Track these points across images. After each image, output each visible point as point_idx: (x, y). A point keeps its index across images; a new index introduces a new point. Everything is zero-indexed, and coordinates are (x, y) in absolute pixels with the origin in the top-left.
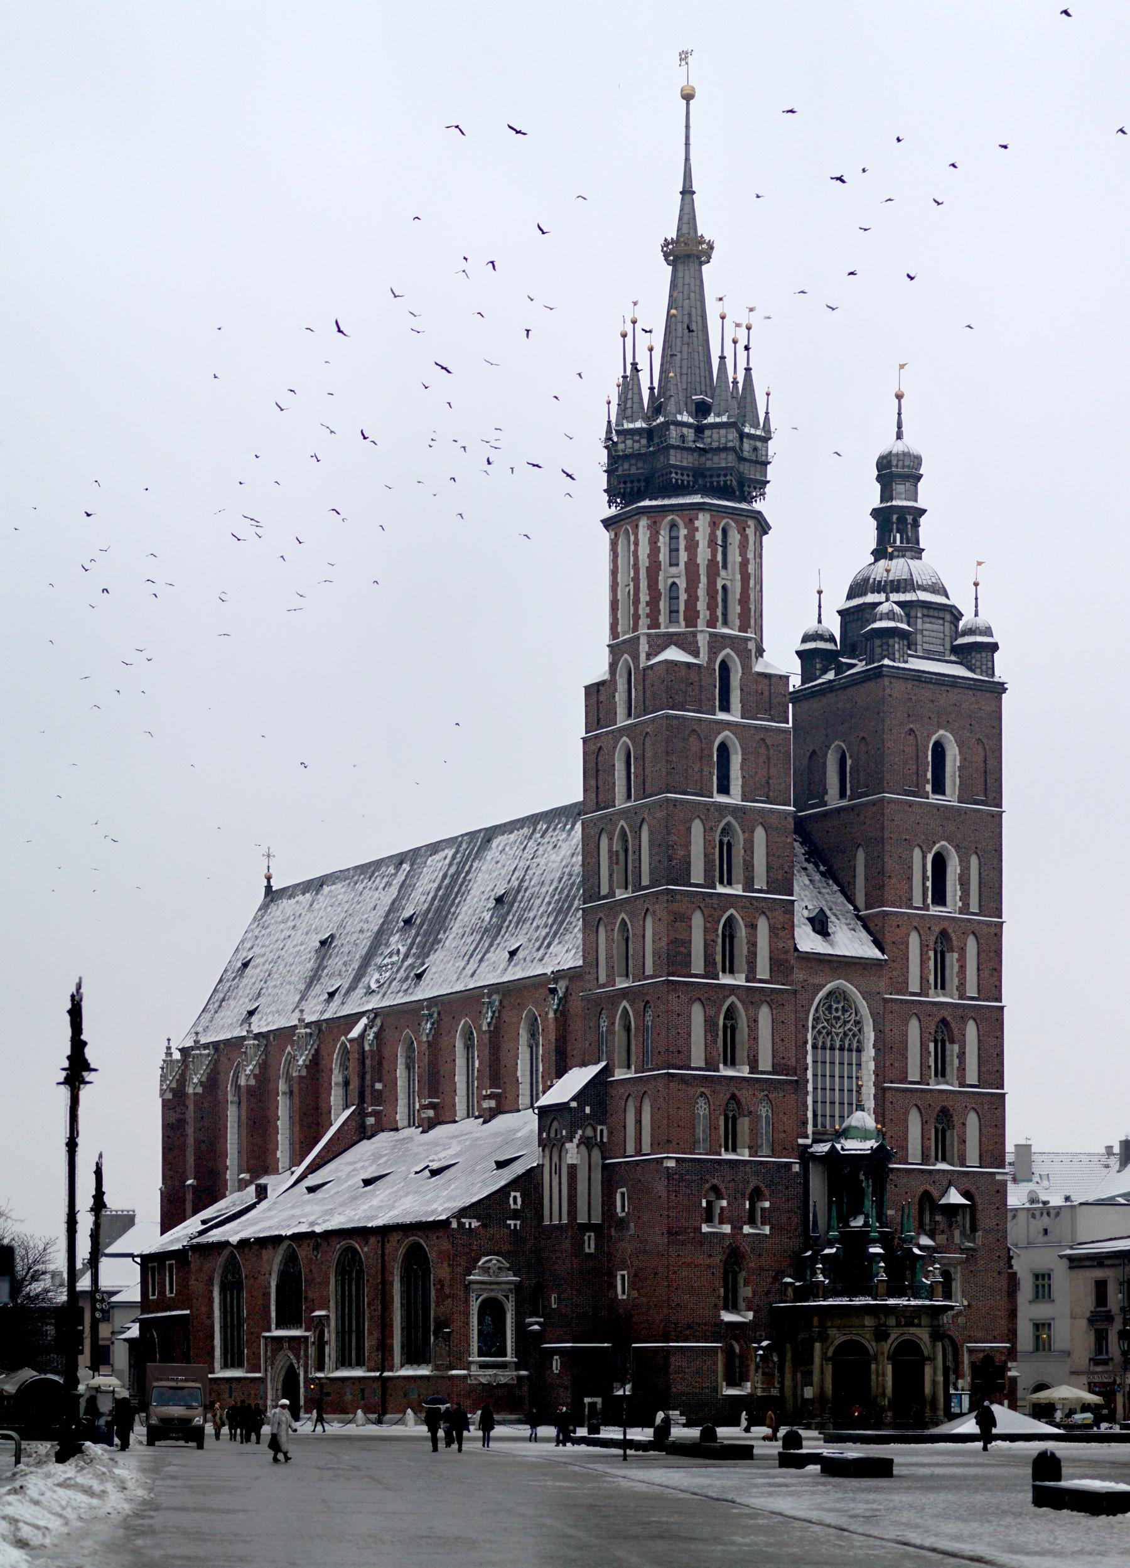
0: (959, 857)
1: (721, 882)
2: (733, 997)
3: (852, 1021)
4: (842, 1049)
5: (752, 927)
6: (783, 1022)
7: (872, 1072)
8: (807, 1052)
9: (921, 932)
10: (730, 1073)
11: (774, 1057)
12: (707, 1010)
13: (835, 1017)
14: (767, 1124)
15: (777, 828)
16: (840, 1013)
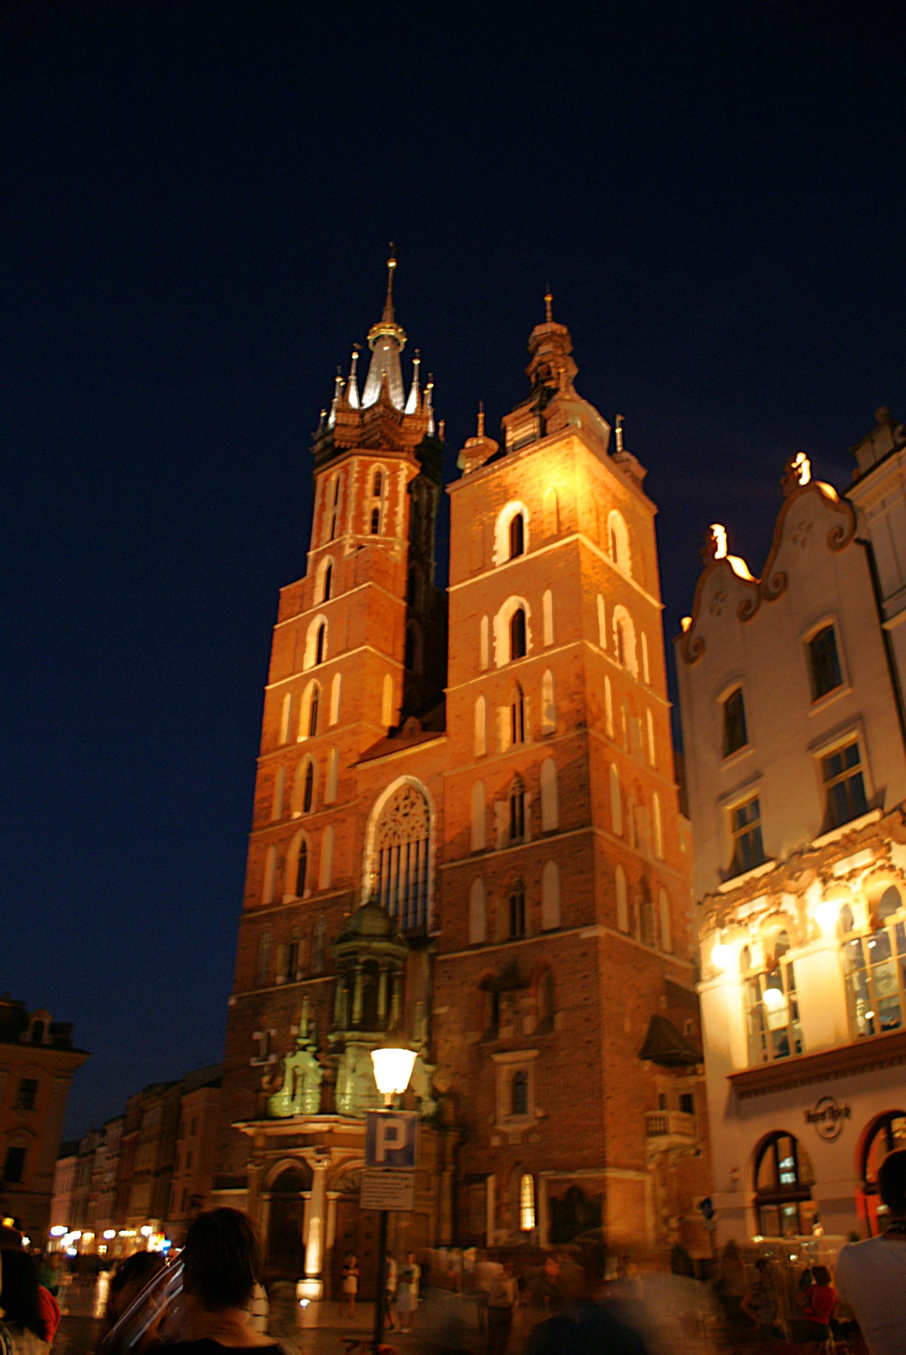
5: (324, 760)
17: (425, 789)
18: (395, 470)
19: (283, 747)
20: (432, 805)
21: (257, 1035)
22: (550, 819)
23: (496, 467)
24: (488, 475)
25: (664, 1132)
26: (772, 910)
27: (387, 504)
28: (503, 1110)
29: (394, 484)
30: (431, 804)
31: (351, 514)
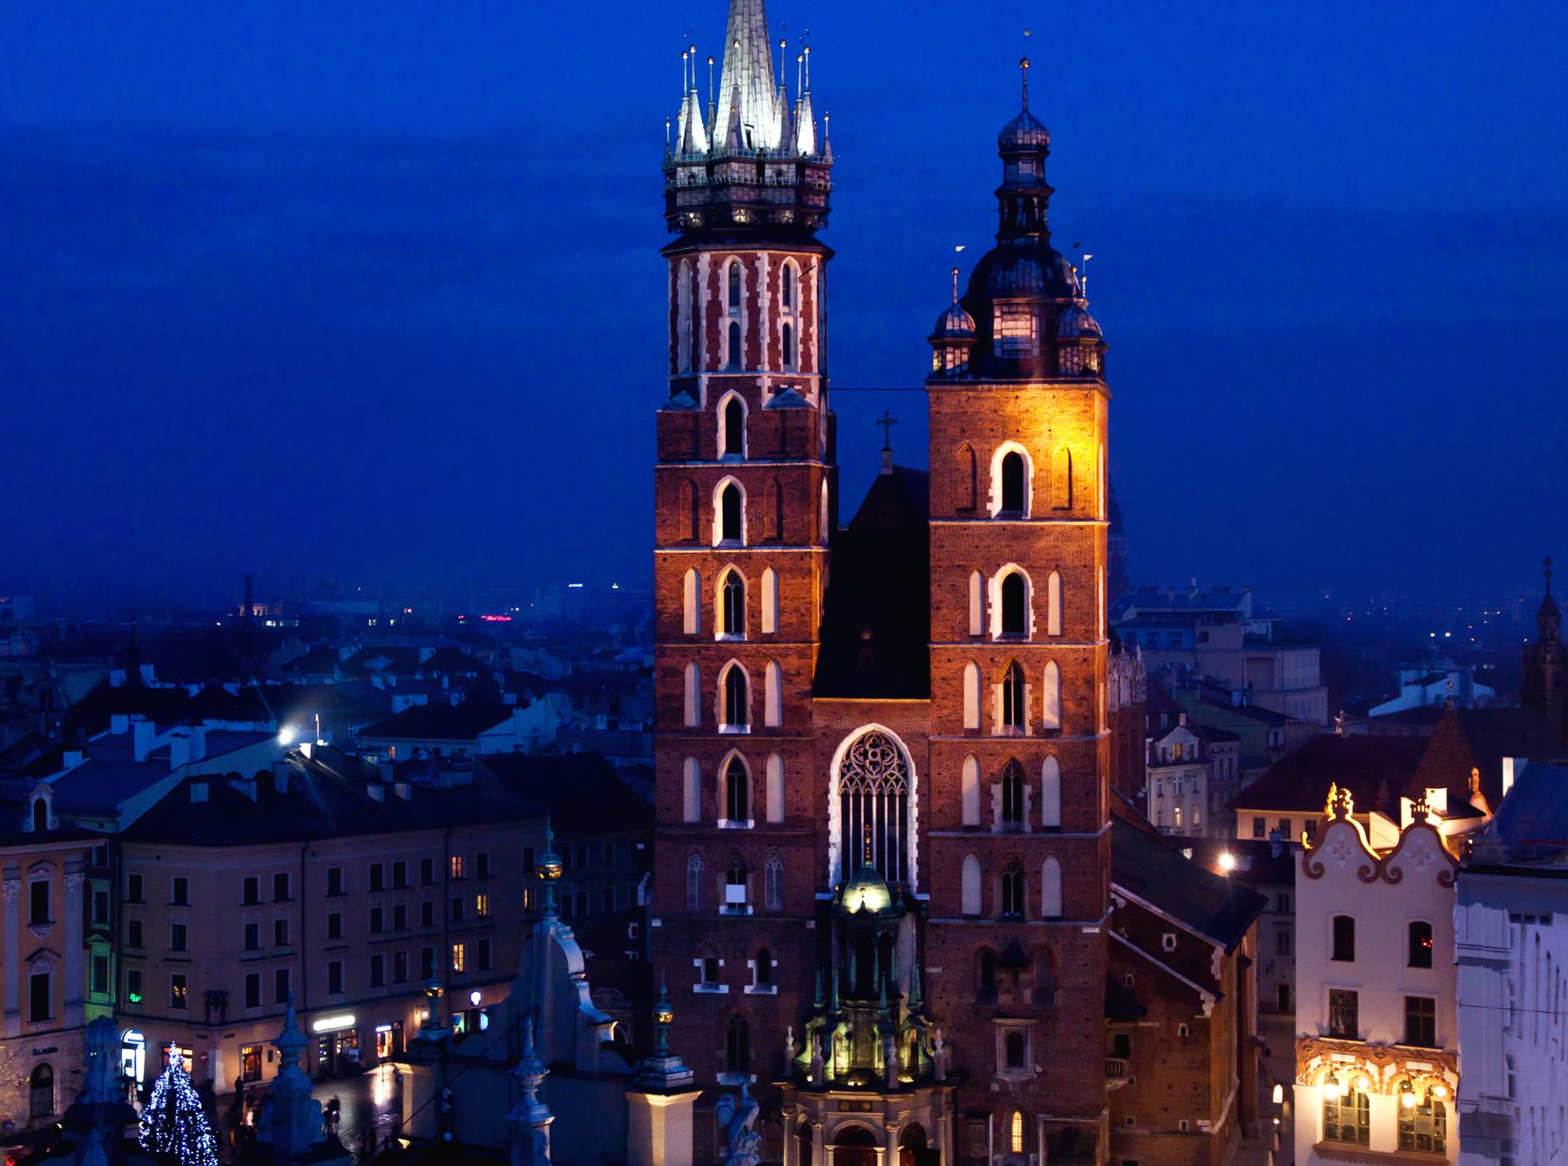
0: (1032, 578)
1: (727, 630)
2: (734, 752)
3: (894, 765)
4: (880, 797)
5: (760, 675)
6: (797, 772)
7: (915, 820)
8: (828, 802)
9: (981, 665)
10: (733, 826)
11: (785, 810)
12: (703, 766)
13: (871, 763)
14: (779, 878)
15: (790, 570)
16: (878, 759)
17: (904, 747)
18: (806, 267)
19: (690, 639)
20: (913, 766)
21: (697, 963)
22: (1051, 813)
23: (994, 387)
24: (982, 390)
25: (1120, 1076)
26: (1359, 1066)
27: (801, 320)
28: (1001, 1063)
29: (807, 290)
30: (913, 766)
31: (766, 340)
